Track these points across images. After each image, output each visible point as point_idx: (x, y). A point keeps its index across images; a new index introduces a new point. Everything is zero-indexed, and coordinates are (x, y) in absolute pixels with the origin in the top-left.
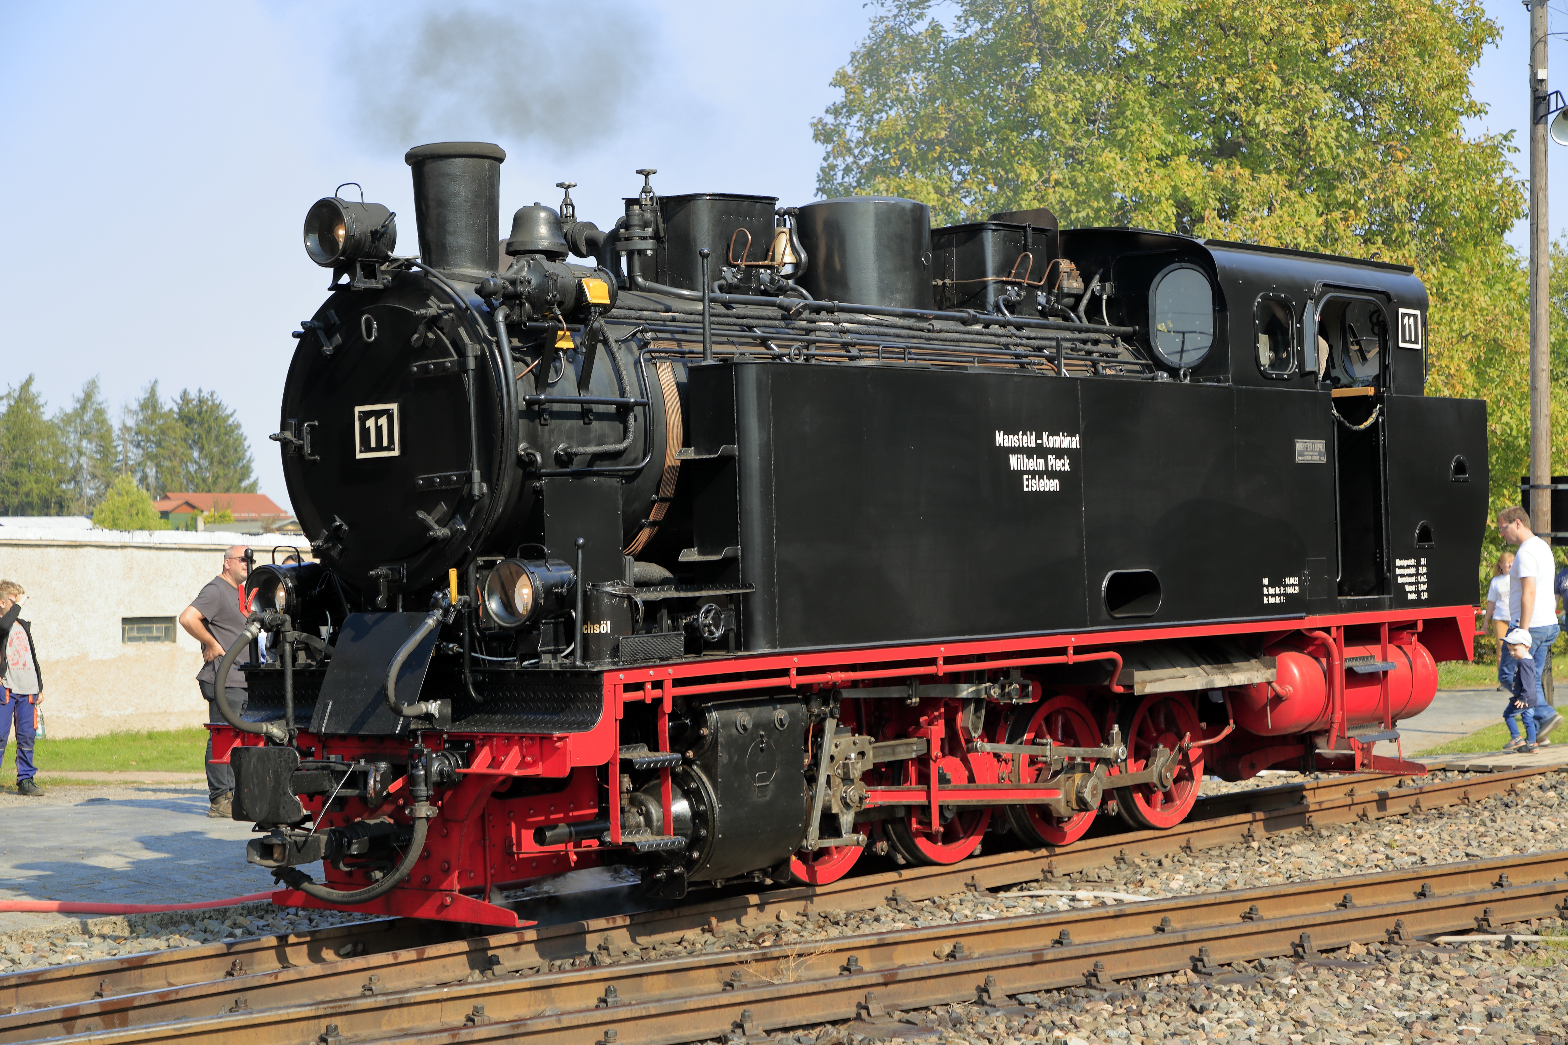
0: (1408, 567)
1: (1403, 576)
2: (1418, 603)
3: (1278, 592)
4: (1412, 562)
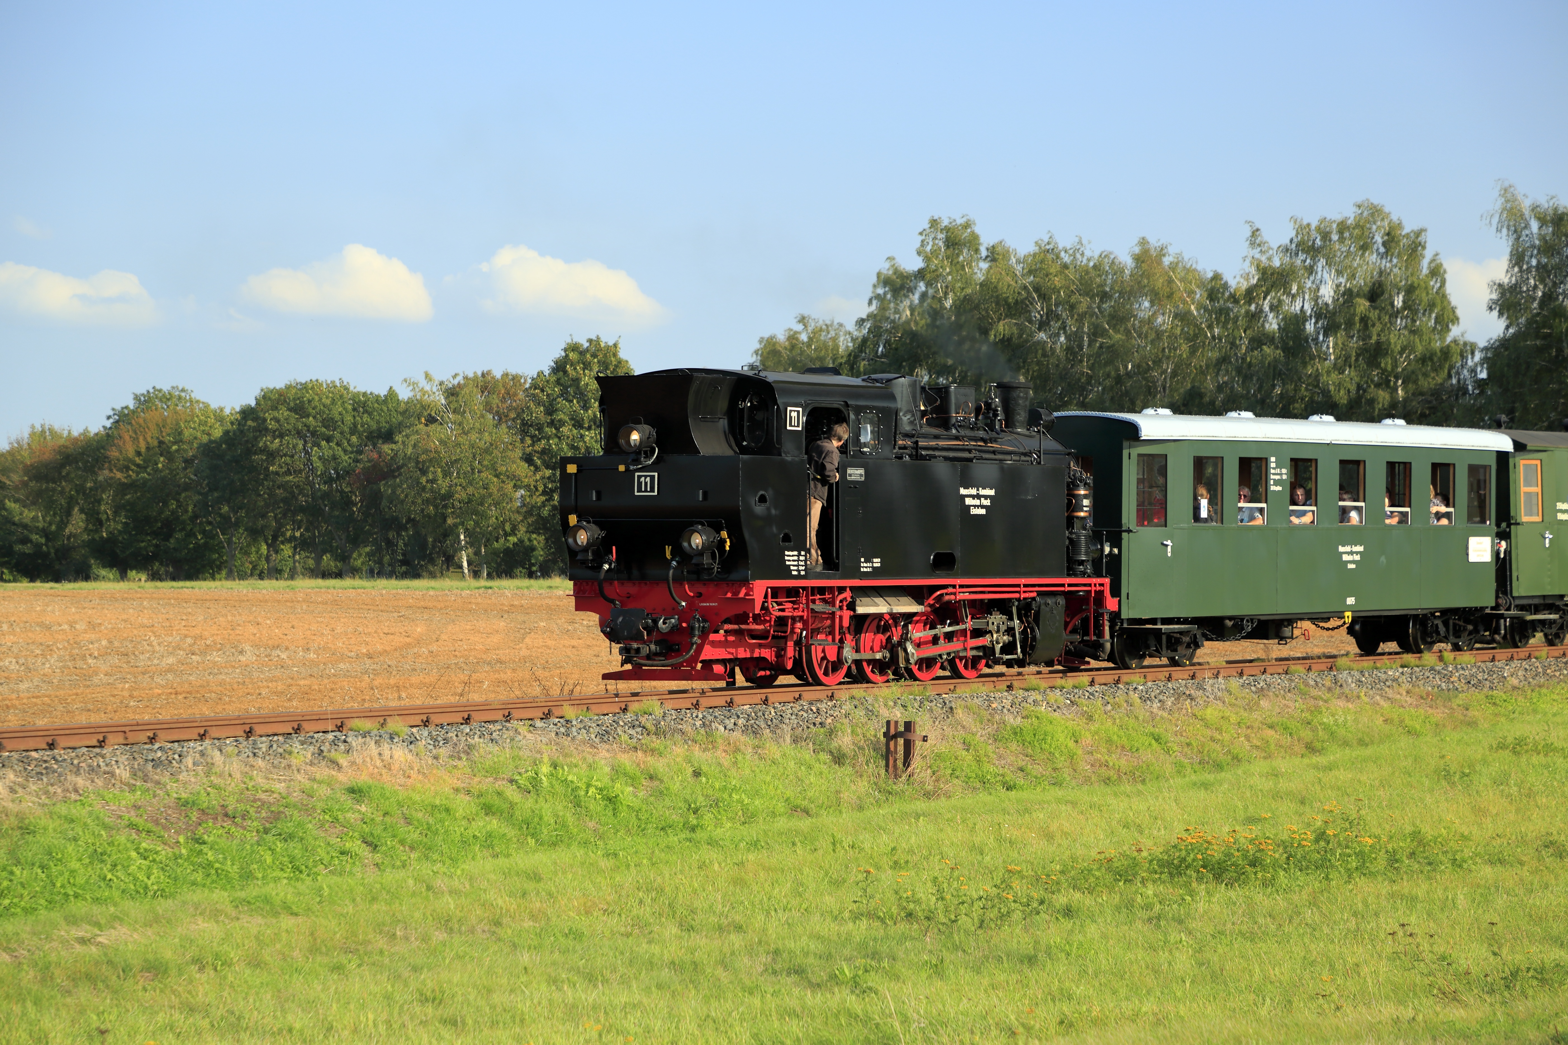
2: (799, 577)
4: (796, 553)
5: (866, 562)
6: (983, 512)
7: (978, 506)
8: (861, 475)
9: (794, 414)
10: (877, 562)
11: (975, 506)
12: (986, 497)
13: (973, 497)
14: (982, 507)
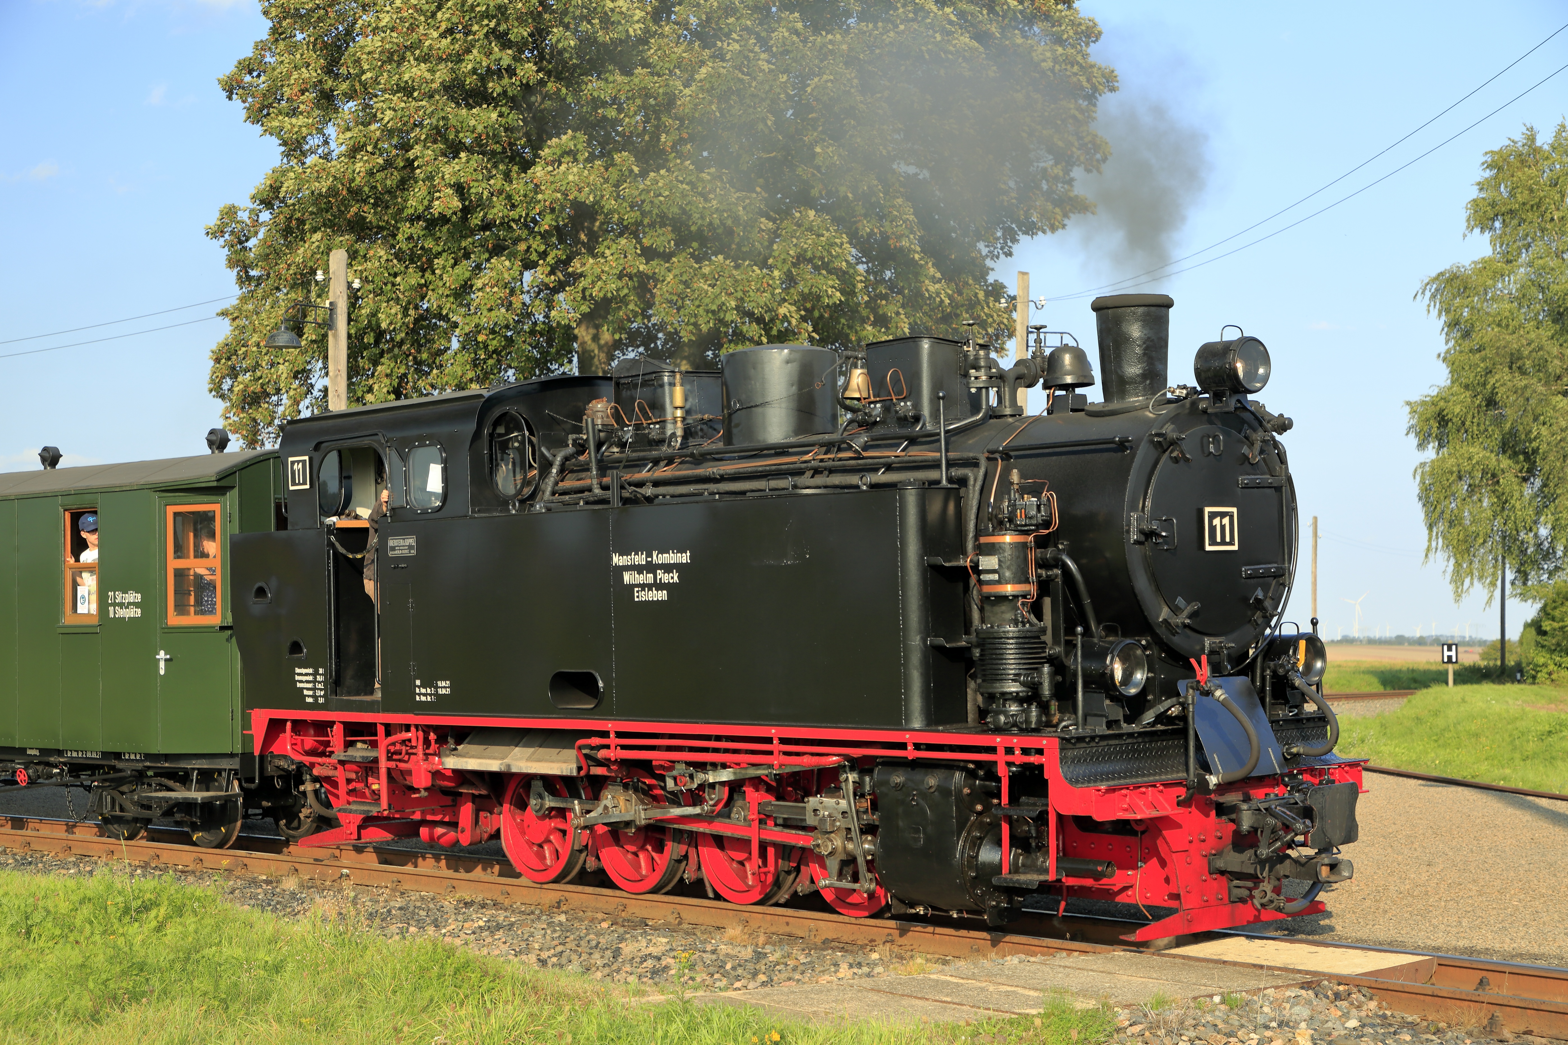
0: (306, 675)
1: (301, 682)
2: (315, 706)
3: (429, 691)
4: (310, 671)
5: (423, 685)
6: (662, 595)
7: (650, 587)
8: (410, 547)
9: (298, 467)
10: (444, 687)
11: (643, 586)
12: (668, 568)
13: (639, 569)
14: (660, 586)
